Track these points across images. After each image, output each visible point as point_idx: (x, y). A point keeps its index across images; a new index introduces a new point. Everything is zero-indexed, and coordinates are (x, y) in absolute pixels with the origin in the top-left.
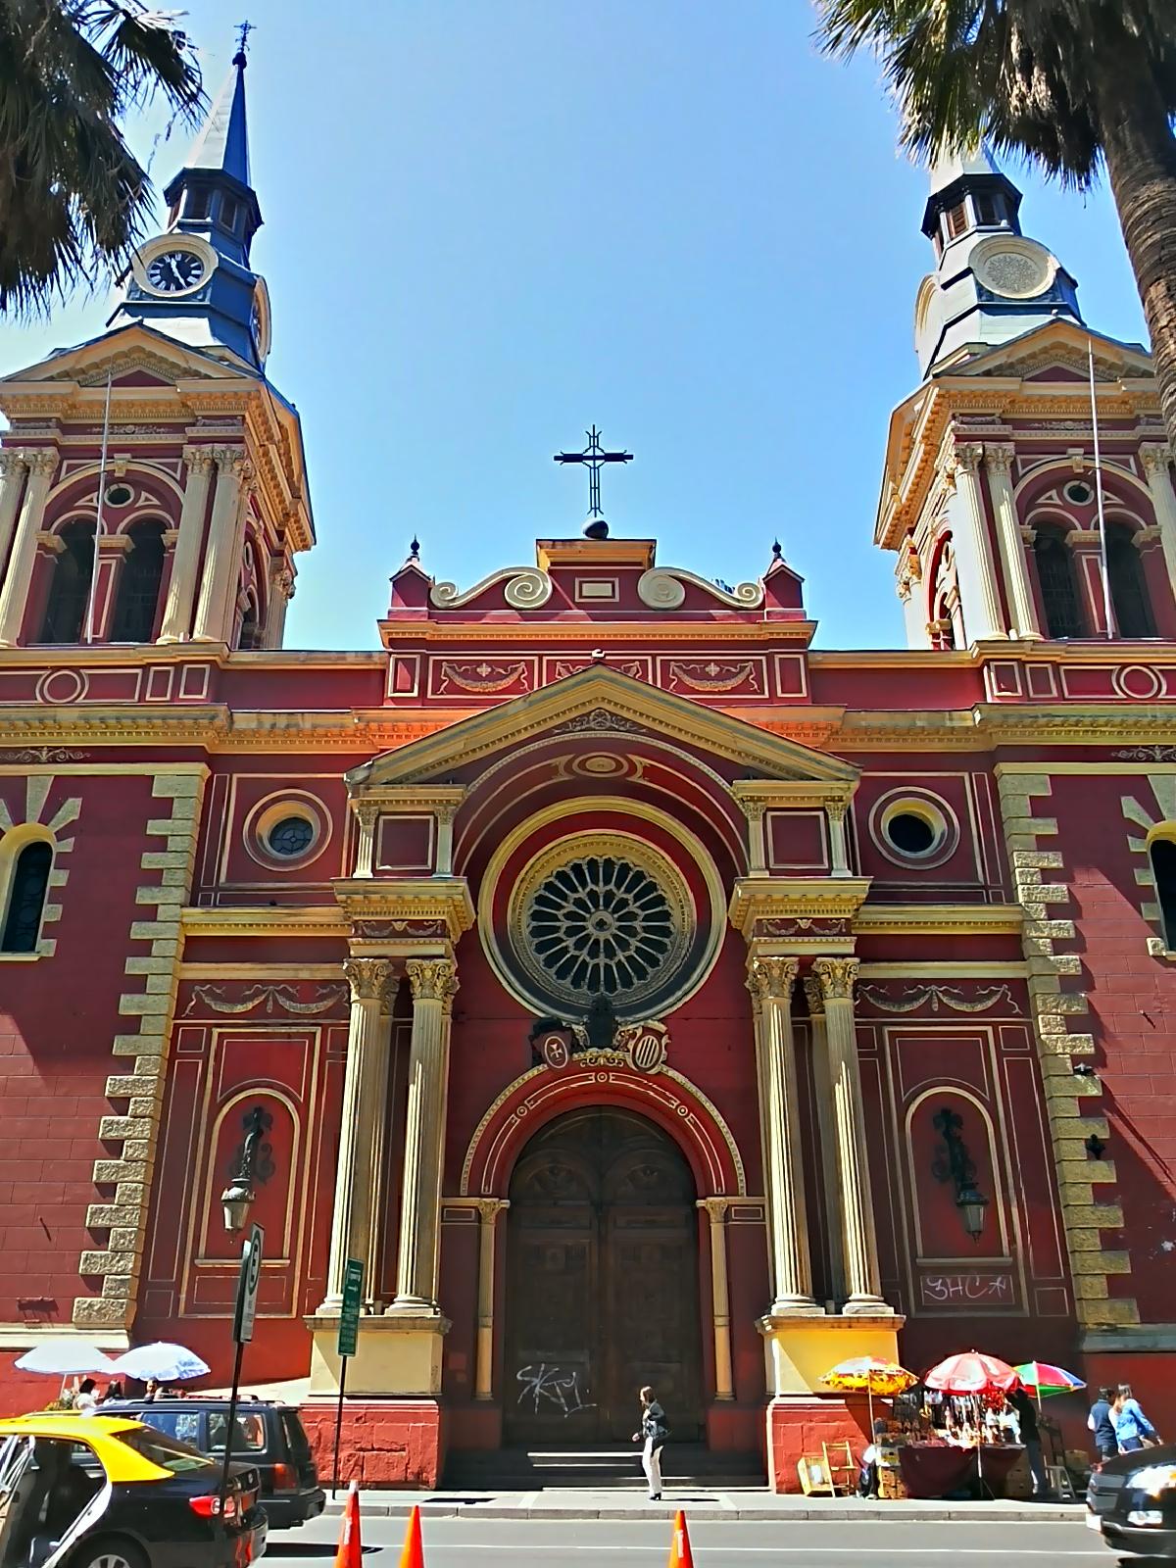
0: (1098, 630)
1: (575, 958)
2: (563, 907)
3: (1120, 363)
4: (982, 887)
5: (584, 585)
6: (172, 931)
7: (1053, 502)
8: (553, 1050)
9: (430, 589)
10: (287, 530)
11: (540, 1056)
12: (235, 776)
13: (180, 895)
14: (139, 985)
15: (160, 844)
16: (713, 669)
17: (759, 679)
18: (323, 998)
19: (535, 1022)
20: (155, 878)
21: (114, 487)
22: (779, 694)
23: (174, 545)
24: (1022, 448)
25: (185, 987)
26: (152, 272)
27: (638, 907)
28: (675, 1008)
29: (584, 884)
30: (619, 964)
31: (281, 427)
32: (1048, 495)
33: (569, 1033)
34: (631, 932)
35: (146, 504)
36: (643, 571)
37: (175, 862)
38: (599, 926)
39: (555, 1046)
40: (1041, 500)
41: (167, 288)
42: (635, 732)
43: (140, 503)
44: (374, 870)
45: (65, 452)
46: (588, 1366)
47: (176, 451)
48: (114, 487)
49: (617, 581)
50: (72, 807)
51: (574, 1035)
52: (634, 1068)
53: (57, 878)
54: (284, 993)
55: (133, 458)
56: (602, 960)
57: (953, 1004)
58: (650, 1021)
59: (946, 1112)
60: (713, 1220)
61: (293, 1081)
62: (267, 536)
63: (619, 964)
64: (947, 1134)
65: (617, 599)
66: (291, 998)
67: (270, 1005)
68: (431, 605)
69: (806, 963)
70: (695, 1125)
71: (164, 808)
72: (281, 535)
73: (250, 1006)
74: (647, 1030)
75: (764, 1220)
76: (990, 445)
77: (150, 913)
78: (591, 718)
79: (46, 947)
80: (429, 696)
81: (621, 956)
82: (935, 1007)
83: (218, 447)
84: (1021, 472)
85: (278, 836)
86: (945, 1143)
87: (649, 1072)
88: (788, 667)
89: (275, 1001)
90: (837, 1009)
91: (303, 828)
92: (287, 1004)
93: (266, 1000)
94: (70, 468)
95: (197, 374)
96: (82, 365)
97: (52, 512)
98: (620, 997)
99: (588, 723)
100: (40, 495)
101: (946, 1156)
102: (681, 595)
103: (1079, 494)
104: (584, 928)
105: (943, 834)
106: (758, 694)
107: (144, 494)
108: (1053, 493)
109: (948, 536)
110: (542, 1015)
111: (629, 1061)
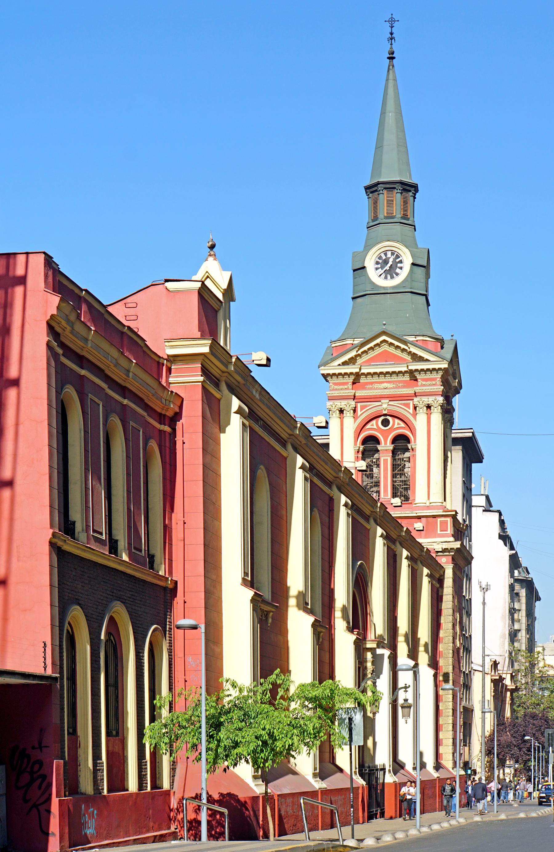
43: (396, 426)
97: (358, 433)
107: (397, 421)
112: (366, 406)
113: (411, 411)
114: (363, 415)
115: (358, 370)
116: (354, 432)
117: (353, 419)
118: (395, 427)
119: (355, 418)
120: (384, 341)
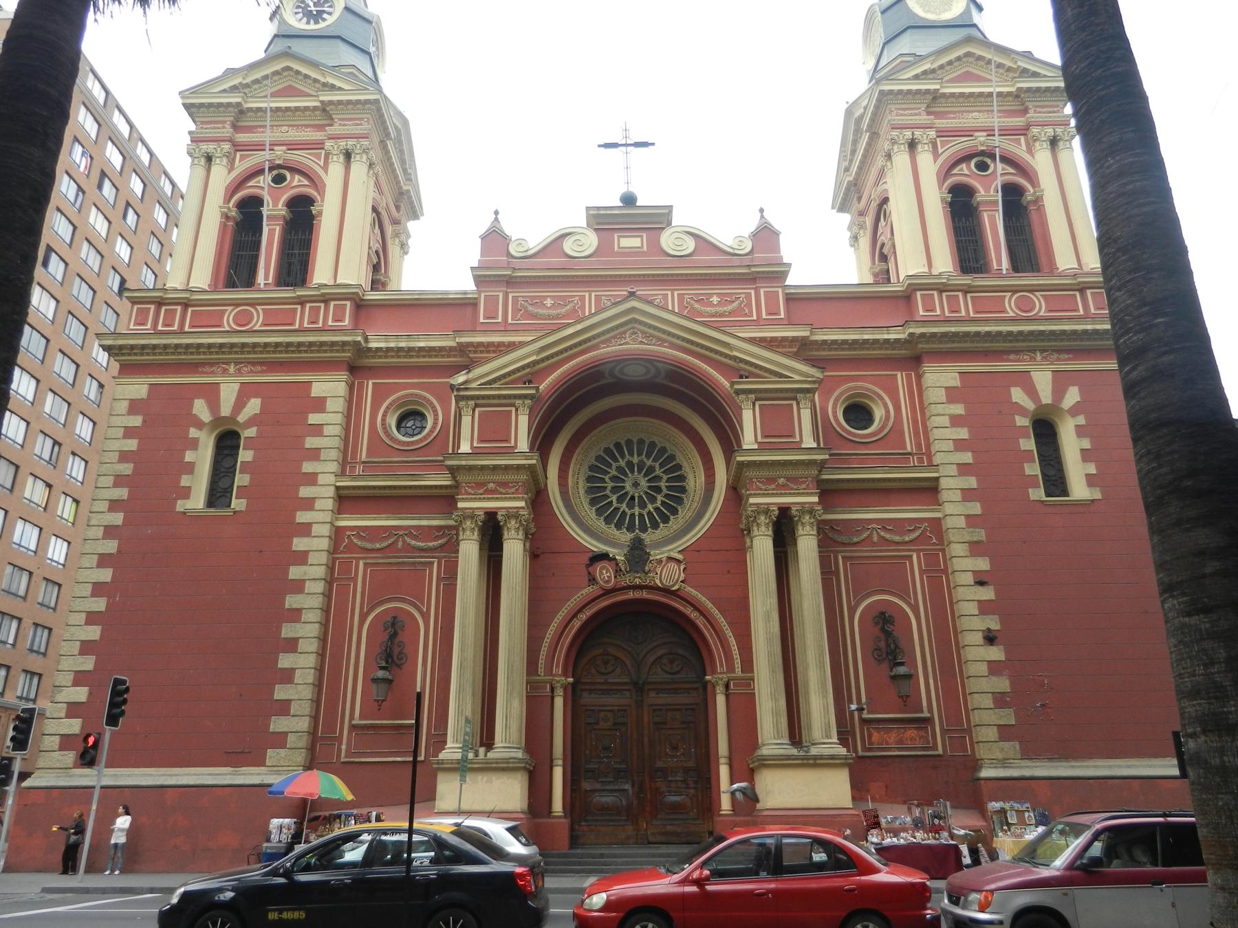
0: (995, 267)
1: (617, 509)
2: (609, 473)
3: (1015, 66)
4: (909, 454)
5: (621, 239)
6: (330, 492)
7: (966, 173)
8: (603, 574)
9: (508, 244)
10: (402, 205)
11: (594, 579)
12: (370, 382)
13: (334, 467)
14: (305, 530)
15: (317, 430)
16: (715, 299)
17: (749, 305)
18: (437, 538)
19: (591, 555)
20: (315, 454)
21: (275, 172)
22: (764, 316)
23: (320, 213)
24: (942, 133)
25: (338, 534)
26: (296, 10)
27: (663, 472)
28: (689, 544)
29: (623, 456)
30: (649, 513)
31: (396, 128)
32: (960, 167)
33: (613, 562)
34: (658, 490)
35: (296, 184)
36: (663, 228)
37: (329, 442)
38: (637, 484)
39: (604, 572)
40: (955, 171)
41: (308, 23)
42: (659, 345)
44: (472, 447)
45: (238, 147)
46: (630, 792)
47: (319, 145)
48: (275, 172)
49: (645, 235)
50: (254, 406)
51: (617, 564)
52: (660, 585)
53: (245, 455)
54: (410, 535)
55: (289, 149)
56: (637, 510)
57: (888, 536)
58: (672, 553)
59: (883, 613)
60: (718, 691)
61: (418, 597)
62: (388, 209)
63: (649, 513)
64: (883, 630)
65: (645, 248)
66: (415, 538)
67: (400, 544)
68: (509, 254)
69: (784, 511)
70: (704, 625)
71: (319, 405)
72: (398, 208)
73: (385, 544)
74: (670, 559)
75: (754, 689)
76: (918, 133)
77: (312, 479)
78: (627, 336)
79: (238, 504)
80: (510, 321)
81: (650, 507)
82: (875, 538)
83: (351, 142)
84: (940, 151)
85: (403, 425)
86: (882, 636)
87: (674, 589)
88: (773, 298)
89: (404, 541)
90: (807, 545)
91: (420, 419)
92: (413, 542)
93: (396, 542)
94: (242, 158)
95: (333, 87)
96: (248, 80)
98: (648, 537)
99: (625, 338)
100: (221, 177)
101: (882, 644)
102: (690, 245)
103: (982, 167)
104: (623, 488)
105: (881, 418)
106: (749, 316)
107: (297, 177)
108: (964, 166)
109: (885, 200)
110: (595, 550)
111: (658, 582)
112: (248, 156)
113: (322, 163)
114: (242, 166)
115: (239, 100)
116: (226, 188)
117: (226, 171)
118: (293, 185)
119: (231, 168)
120: (288, 68)
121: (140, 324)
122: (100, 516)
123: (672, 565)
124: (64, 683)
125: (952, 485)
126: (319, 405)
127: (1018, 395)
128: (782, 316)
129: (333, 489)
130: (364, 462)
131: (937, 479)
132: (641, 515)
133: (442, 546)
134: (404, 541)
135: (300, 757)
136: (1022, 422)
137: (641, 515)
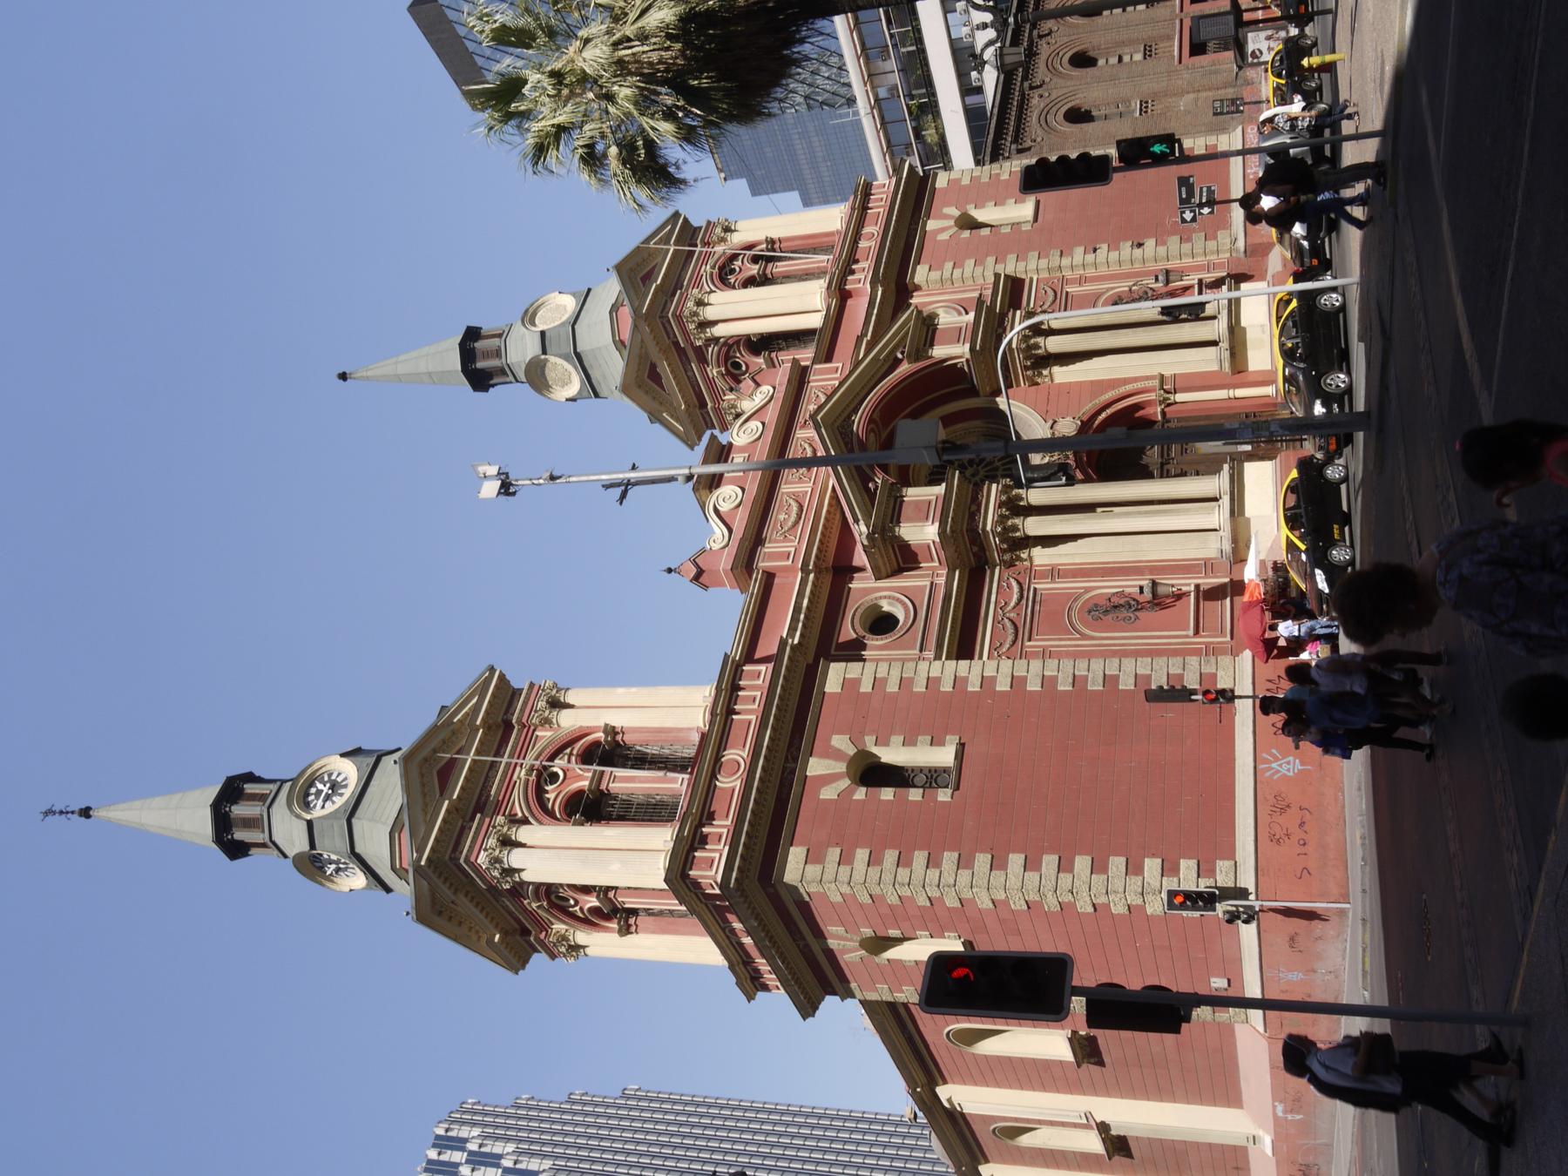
12: (833, 652)
18: (1009, 586)
74: (1052, 428)
87: (1079, 423)
89: (1010, 612)
93: (1010, 620)
121: (711, 866)
122: (945, 874)
123: (1057, 427)
124: (1140, 883)
125: (1011, 267)
126: (849, 685)
127: (944, 236)
128: (841, 365)
129: (948, 663)
130: (921, 651)
131: (1005, 275)
132: (1004, 470)
133: (1019, 583)
134: (1010, 612)
135: (1225, 660)
136: (966, 234)
137: (1004, 470)
